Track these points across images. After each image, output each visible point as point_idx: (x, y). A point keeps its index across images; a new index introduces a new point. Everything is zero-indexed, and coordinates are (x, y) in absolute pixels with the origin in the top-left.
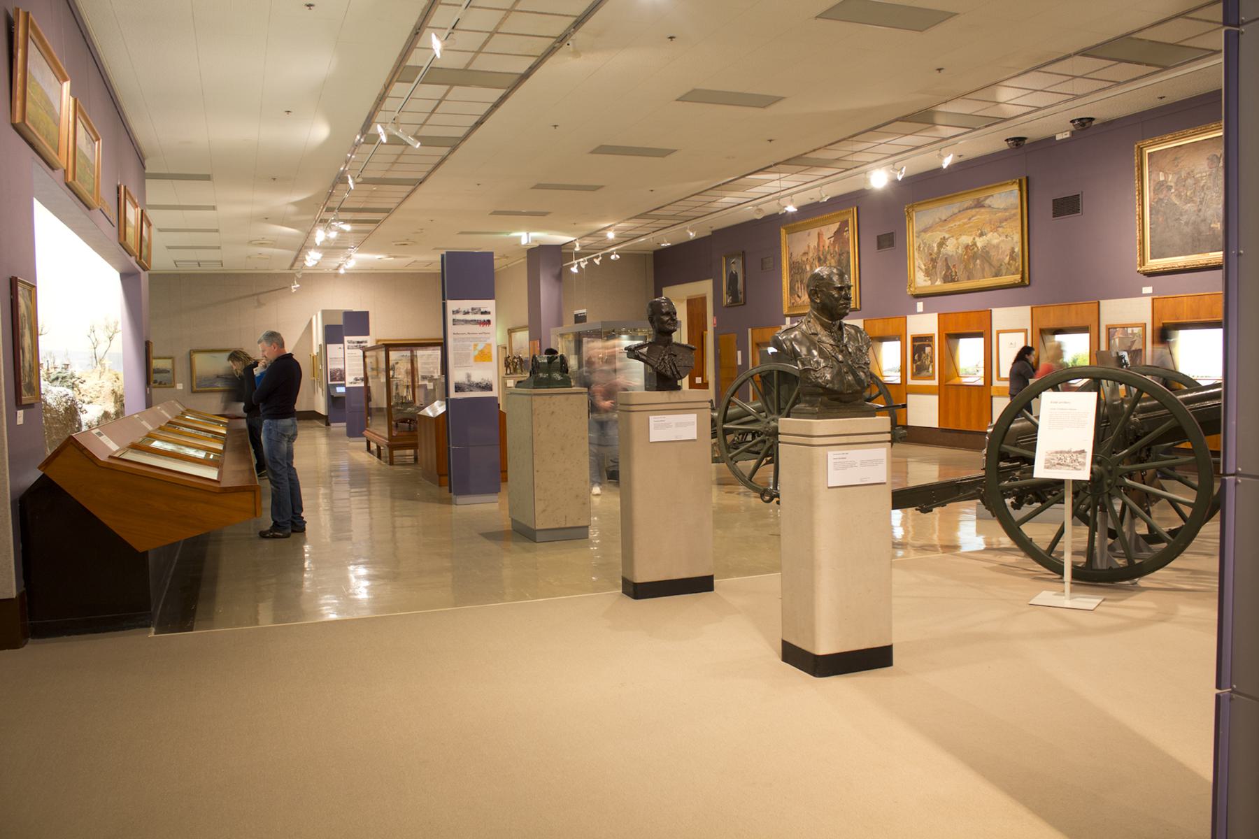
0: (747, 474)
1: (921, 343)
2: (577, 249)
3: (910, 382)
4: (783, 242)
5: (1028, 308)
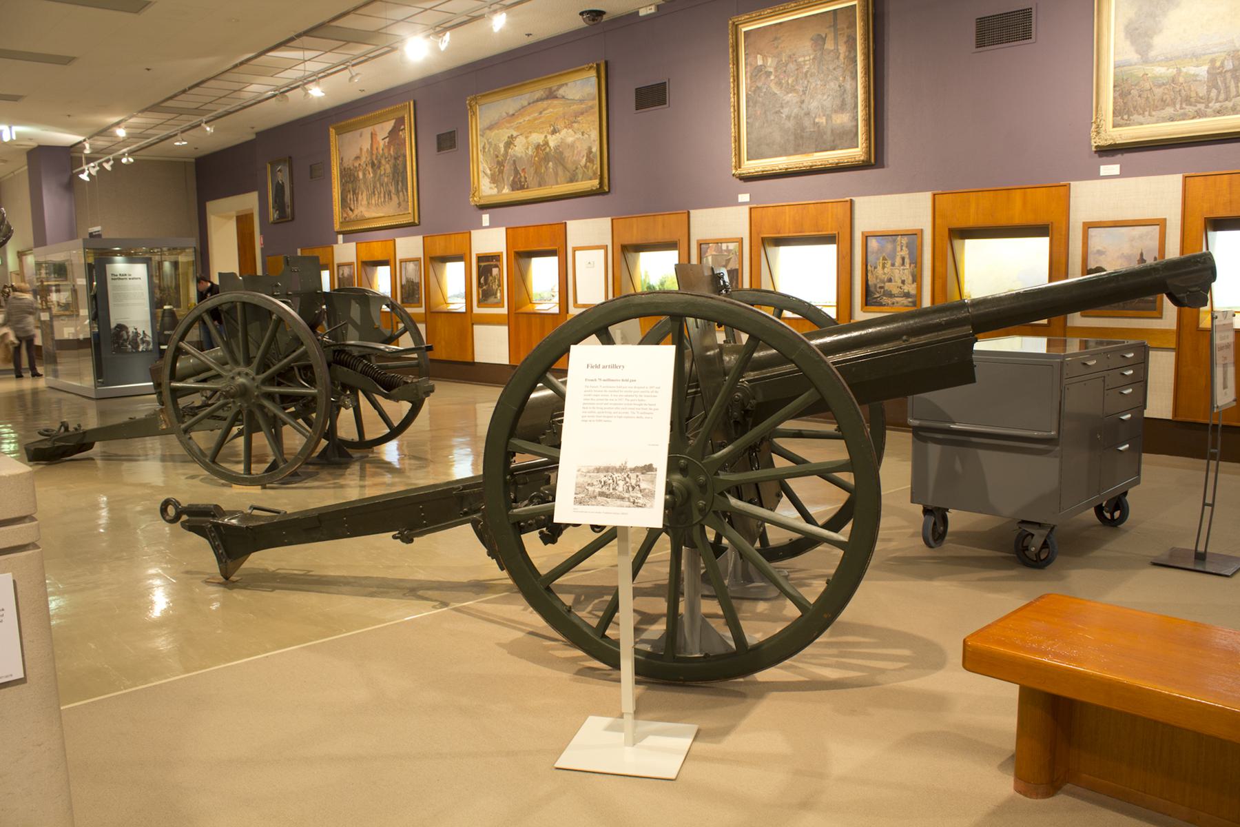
0: (209, 453)
1: (487, 263)
2: (87, 151)
3: (477, 310)
4: (333, 144)
5: (609, 219)
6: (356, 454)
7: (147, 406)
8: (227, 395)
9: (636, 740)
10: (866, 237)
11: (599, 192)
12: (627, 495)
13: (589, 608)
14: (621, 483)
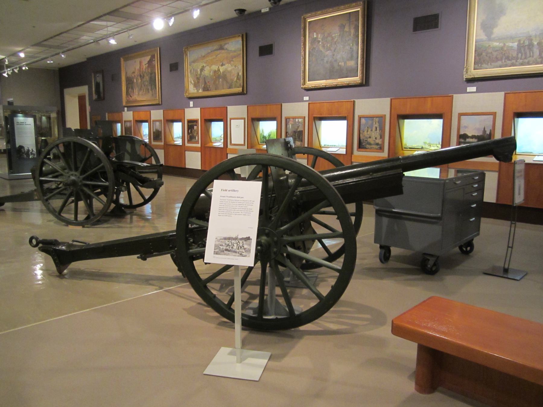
0: (58, 210)
1: (192, 124)
2: (7, 63)
3: (187, 144)
4: (122, 65)
5: (246, 106)
6: (128, 211)
7: (30, 186)
8: (66, 185)
9: (241, 360)
10: (360, 118)
11: (242, 94)
12: (238, 251)
13: (227, 291)
14: (235, 245)
